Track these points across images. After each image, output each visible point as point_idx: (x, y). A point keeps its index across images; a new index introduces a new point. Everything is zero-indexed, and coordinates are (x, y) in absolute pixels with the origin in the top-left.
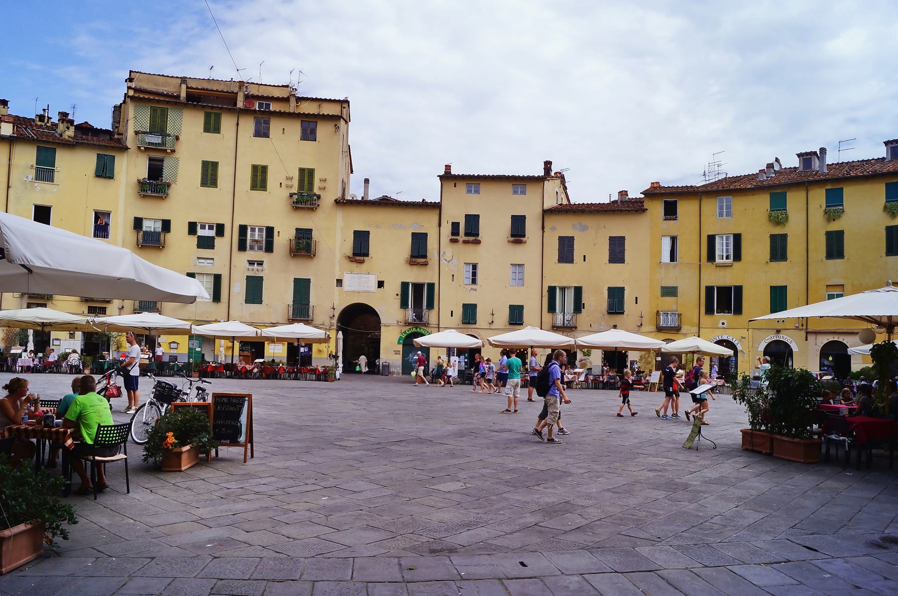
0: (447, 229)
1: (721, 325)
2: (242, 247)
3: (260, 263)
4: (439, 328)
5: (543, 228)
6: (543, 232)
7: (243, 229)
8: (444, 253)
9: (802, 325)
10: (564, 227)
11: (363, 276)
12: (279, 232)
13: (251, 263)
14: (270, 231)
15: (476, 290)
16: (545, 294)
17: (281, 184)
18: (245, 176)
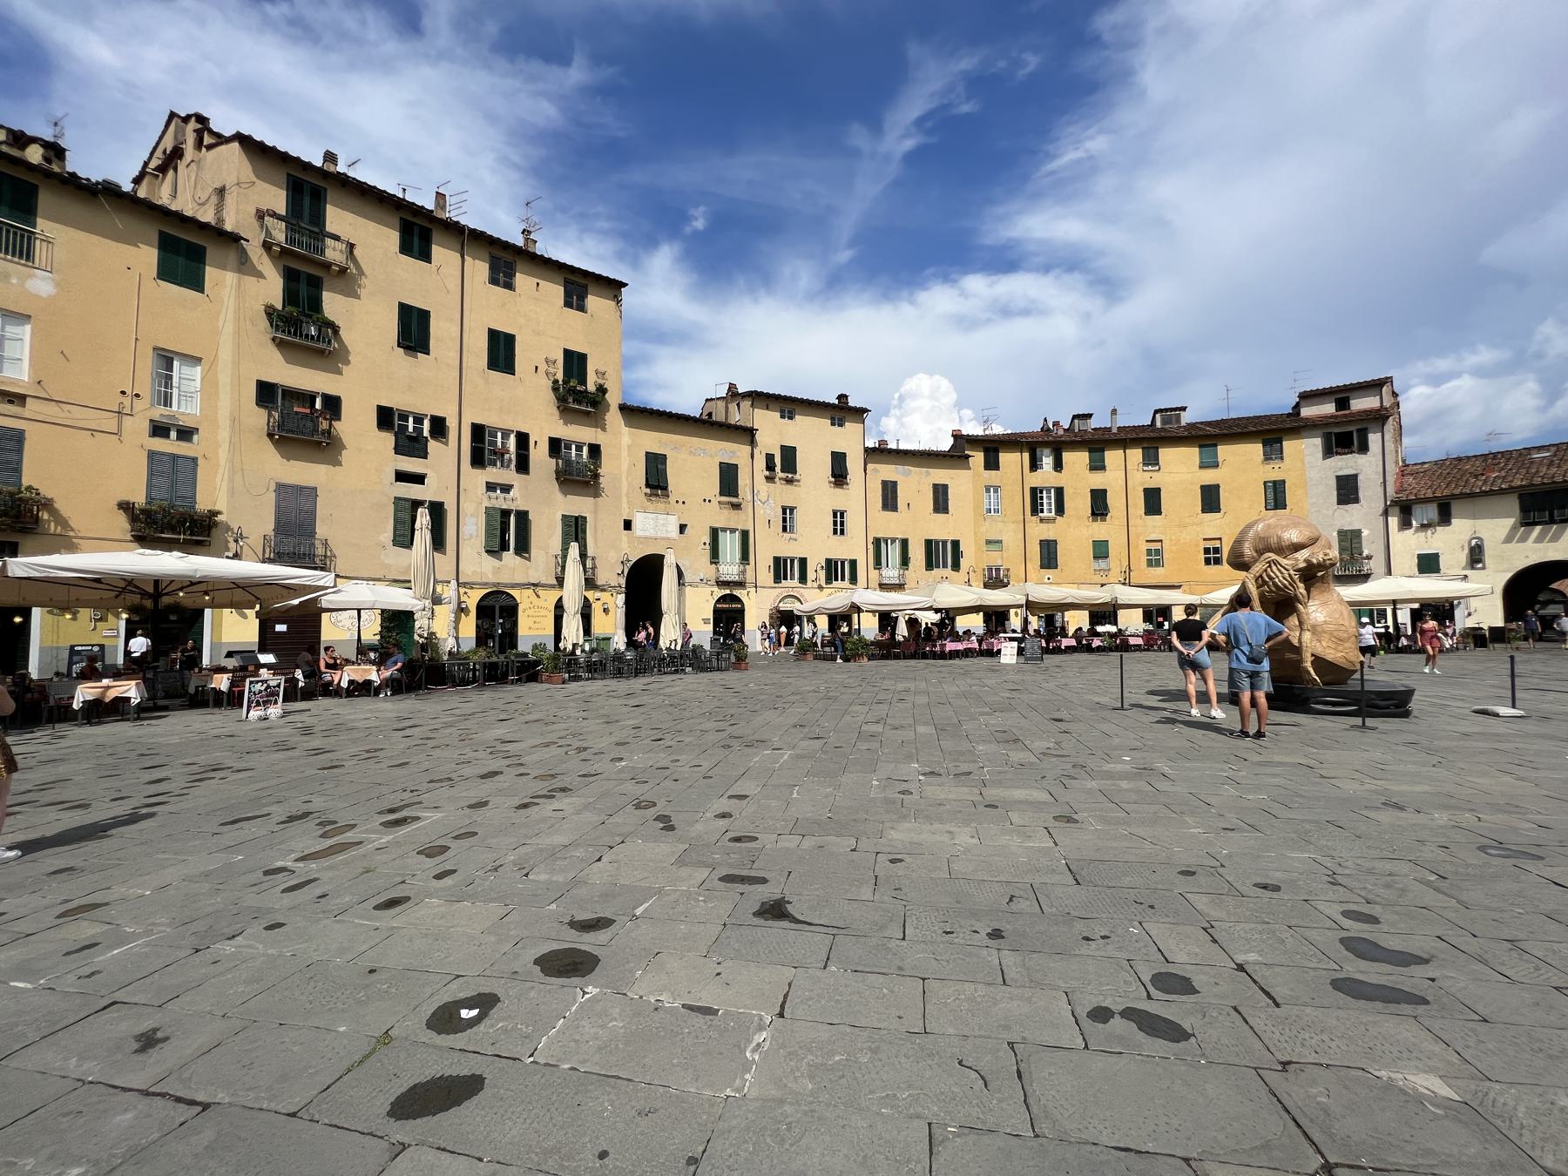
0: (761, 463)
1: (1046, 580)
2: (478, 460)
3: (506, 489)
4: (756, 587)
5: (865, 470)
6: (866, 474)
7: (478, 431)
8: (758, 491)
9: (1125, 579)
10: (888, 471)
11: (660, 516)
12: (536, 442)
13: (491, 487)
14: (523, 439)
15: (796, 540)
16: (871, 547)
17: (537, 367)
18: (479, 347)
